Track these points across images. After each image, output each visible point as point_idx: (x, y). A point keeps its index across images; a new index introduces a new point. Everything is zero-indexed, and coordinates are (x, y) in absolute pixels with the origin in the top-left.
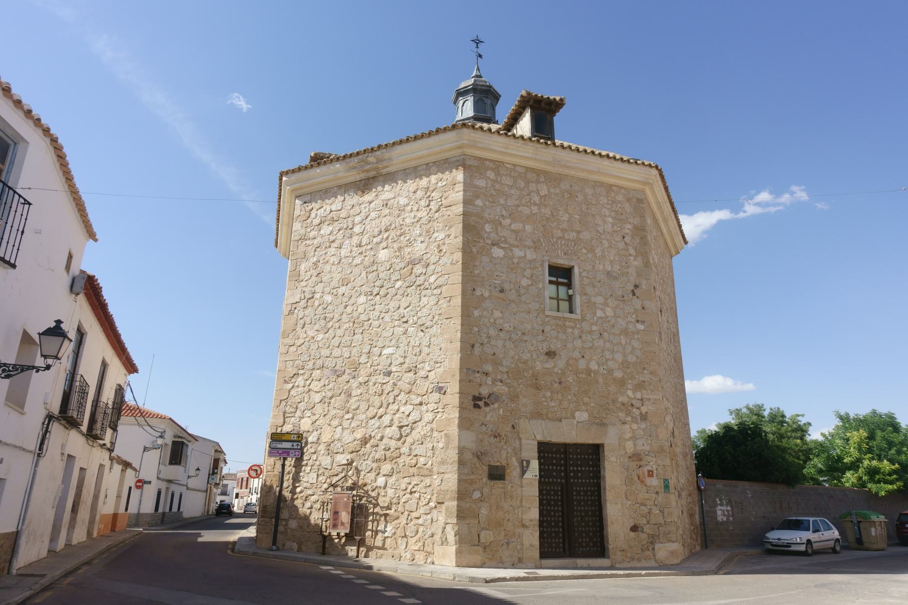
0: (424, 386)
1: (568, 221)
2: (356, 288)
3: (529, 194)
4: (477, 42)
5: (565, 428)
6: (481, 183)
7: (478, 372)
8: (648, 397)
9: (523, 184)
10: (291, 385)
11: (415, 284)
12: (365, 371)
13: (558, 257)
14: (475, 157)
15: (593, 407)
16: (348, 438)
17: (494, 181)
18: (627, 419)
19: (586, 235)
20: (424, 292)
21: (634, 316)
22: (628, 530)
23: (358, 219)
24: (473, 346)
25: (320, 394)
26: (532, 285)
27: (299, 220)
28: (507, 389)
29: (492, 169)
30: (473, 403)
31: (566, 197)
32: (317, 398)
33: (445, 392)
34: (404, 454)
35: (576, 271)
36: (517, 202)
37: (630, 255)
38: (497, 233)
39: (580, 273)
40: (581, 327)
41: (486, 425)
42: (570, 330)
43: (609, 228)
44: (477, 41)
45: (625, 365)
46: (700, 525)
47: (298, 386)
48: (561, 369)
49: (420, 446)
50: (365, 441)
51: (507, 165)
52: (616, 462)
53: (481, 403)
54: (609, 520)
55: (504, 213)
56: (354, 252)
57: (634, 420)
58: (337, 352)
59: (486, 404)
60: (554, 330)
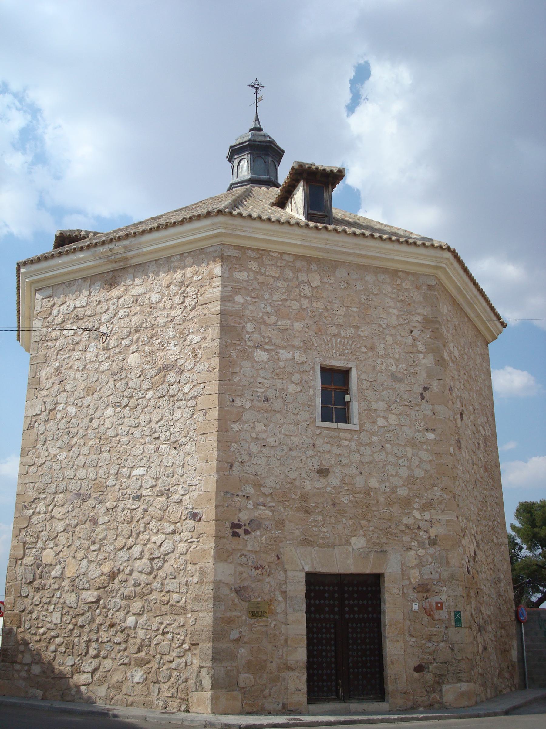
0: (178, 512)
1: (344, 315)
2: (103, 399)
3: (298, 286)
4: (257, 87)
5: (338, 556)
6: (241, 276)
7: (238, 495)
8: (438, 517)
9: (291, 275)
10: (31, 511)
11: (168, 394)
12: (113, 496)
13: (332, 358)
14: (234, 246)
15: (373, 531)
16: (94, 572)
17: (257, 272)
18: (413, 544)
19: (365, 331)
20: (177, 404)
21: (422, 424)
22: (412, 671)
23: (105, 318)
24: (232, 466)
25: (63, 522)
26: (301, 391)
27: (39, 318)
28: (271, 514)
29: (255, 259)
30: (231, 531)
31: (343, 287)
32: (60, 526)
33: (200, 518)
34: (156, 590)
35: (354, 374)
36: (284, 296)
37: (419, 352)
38: (260, 334)
39: (359, 375)
40: (360, 438)
41: (246, 556)
42: (345, 443)
43: (393, 320)
44: (257, 86)
45: (411, 481)
46: (519, 662)
47: (39, 513)
48: (334, 488)
49: (173, 581)
50: (113, 575)
51: (273, 254)
52: (398, 594)
53: (240, 531)
55: (269, 309)
56: (100, 356)
57: (421, 545)
58: (82, 473)
59: (247, 532)
60: (327, 443)
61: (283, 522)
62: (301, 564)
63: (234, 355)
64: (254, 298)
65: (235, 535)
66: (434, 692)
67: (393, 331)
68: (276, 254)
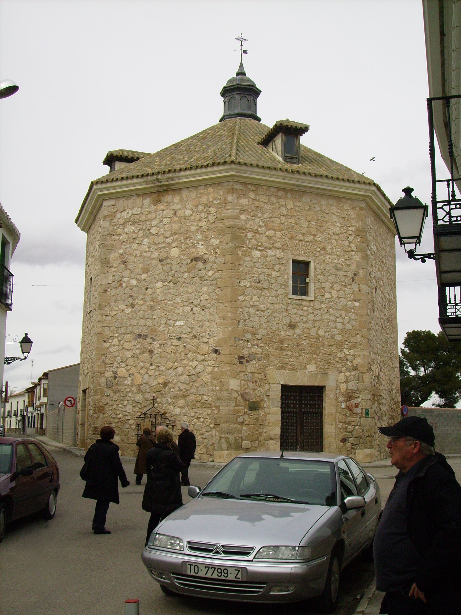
2: (155, 276)
5: (299, 376)
8: (358, 354)
17: (254, 200)
18: (343, 369)
19: (319, 238)
26: (280, 276)
30: (239, 361)
33: (220, 353)
35: (312, 265)
36: (271, 215)
40: (314, 305)
45: (343, 331)
52: (333, 398)
58: (142, 322)
59: (248, 361)
64: (252, 216)
65: (241, 363)
66: (351, 454)
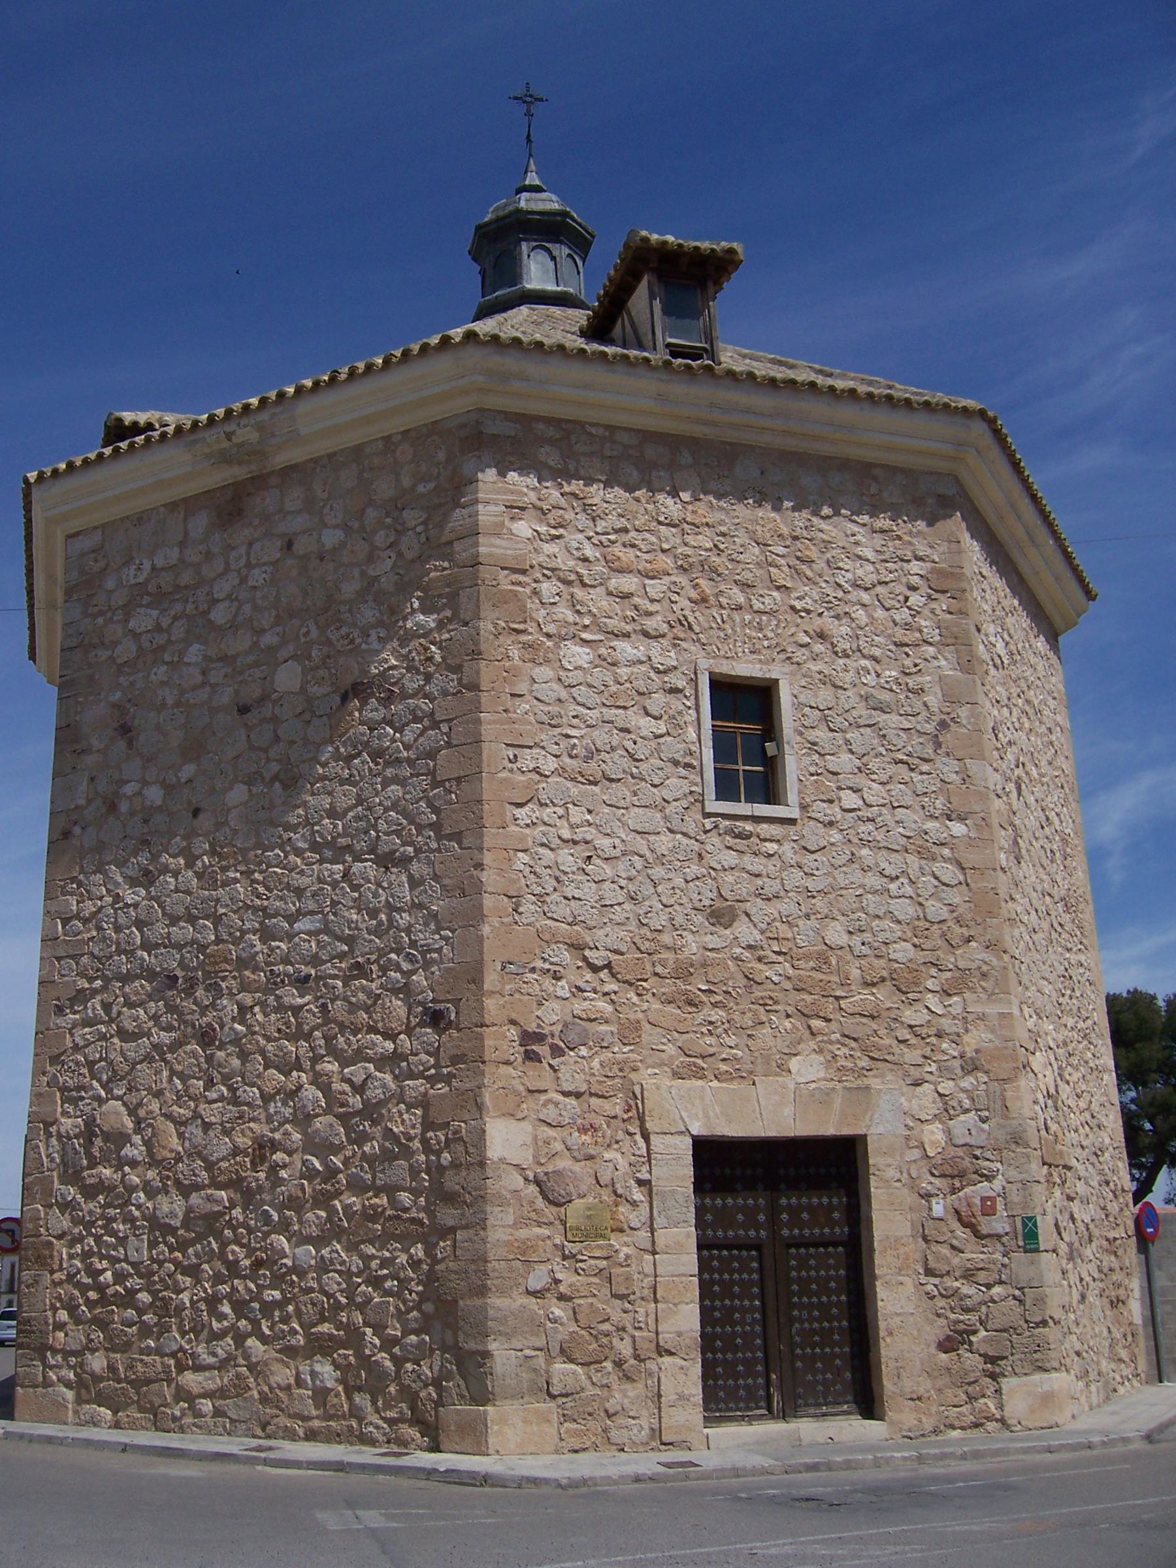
13: (735, 658)
14: (505, 413)
18: (928, 1069)
19: (807, 596)
29: (551, 442)
30: (522, 1049)
36: (621, 523)
41: (557, 1104)
45: (918, 930)
46: (1145, 1325)
51: (593, 431)
52: (899, 1180)
53: (543, 1050)
54: (882, 1325)
59: (557, 1051)
61: (636, 1026)
62: (682, 1117)
63: (515, 653)
64: (554, 528)
65: (531, 1057)
66: (983, 1396)
67: (865, 597)
68: (601, 431)
